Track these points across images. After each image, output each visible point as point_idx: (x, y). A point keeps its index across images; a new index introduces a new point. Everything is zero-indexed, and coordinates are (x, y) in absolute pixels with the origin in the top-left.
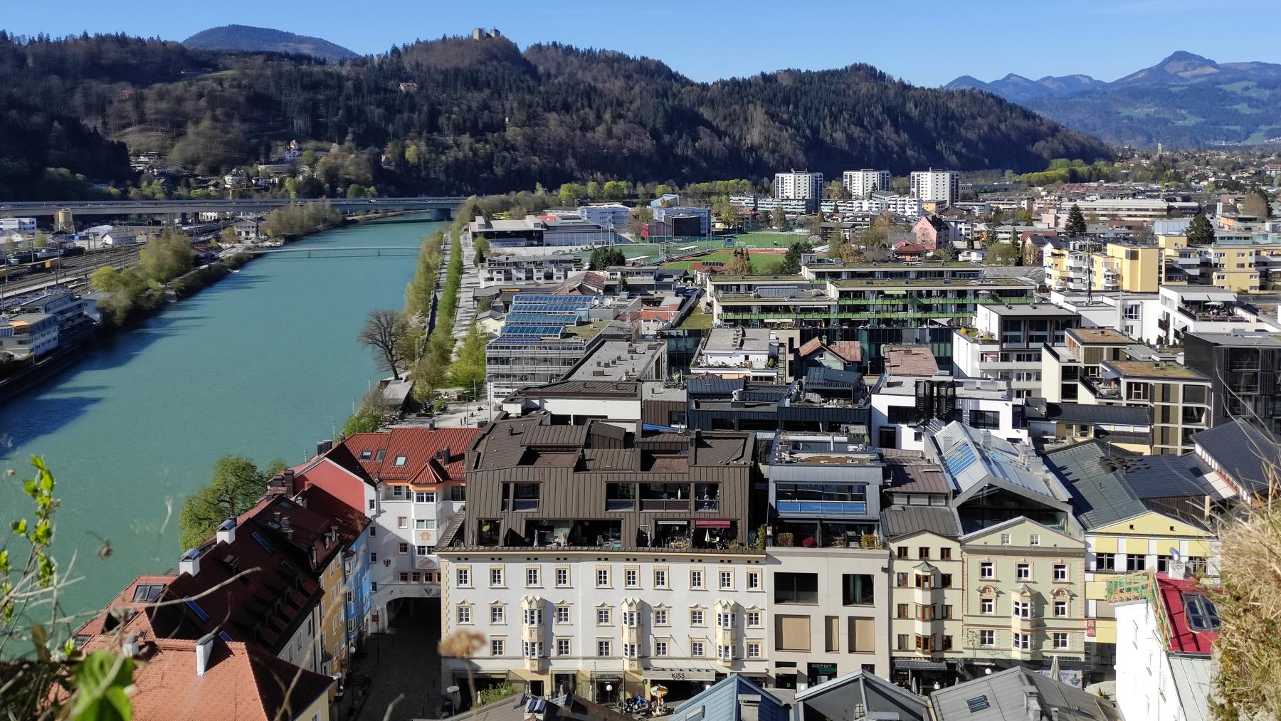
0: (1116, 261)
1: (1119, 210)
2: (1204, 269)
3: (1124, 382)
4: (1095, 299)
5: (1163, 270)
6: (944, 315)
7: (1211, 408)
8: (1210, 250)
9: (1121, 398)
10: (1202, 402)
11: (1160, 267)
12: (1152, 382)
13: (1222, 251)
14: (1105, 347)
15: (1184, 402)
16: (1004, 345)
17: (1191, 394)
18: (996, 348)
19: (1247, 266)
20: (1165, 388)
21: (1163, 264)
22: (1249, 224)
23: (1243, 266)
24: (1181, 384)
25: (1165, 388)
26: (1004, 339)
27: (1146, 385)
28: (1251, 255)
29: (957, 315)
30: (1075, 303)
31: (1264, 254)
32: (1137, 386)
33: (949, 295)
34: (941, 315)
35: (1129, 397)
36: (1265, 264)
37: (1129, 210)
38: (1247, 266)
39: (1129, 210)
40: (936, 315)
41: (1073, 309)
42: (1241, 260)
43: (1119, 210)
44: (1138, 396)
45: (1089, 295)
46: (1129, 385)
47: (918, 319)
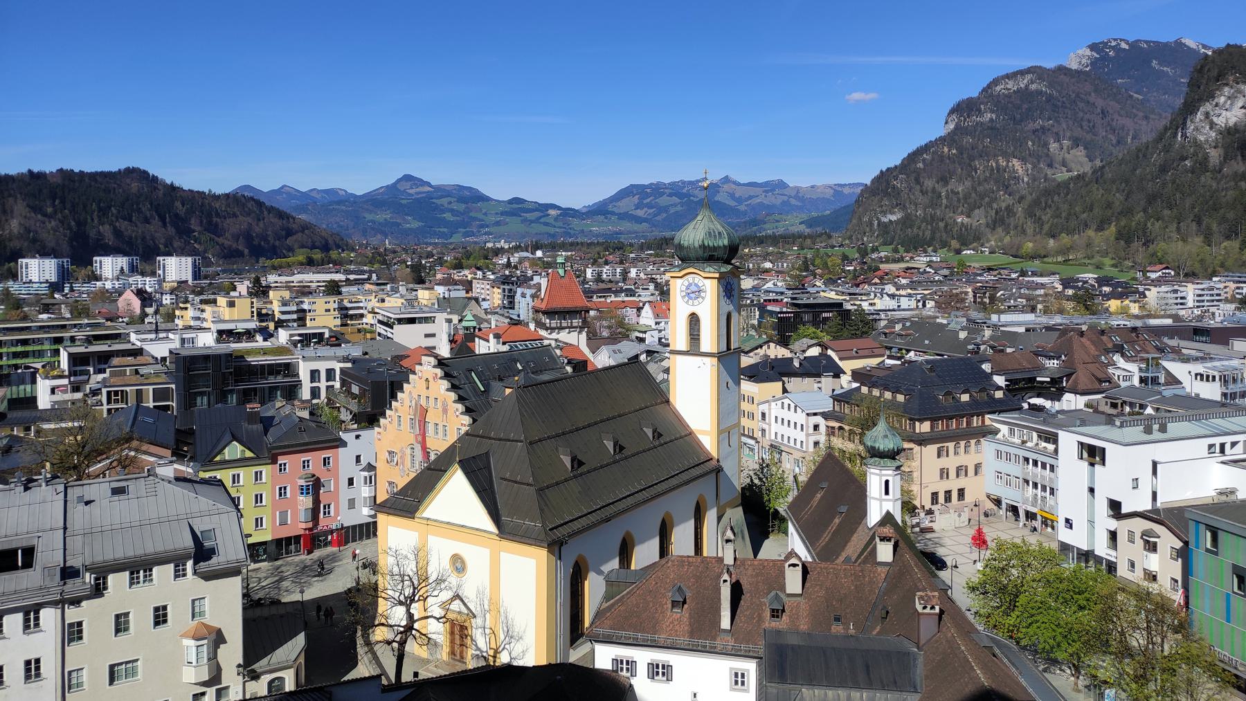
0: (221, 309)
1: (311, 282)
2: (301, 315)
3: (104, 391)
4: (162, 335)
5: (255, 314)
6: (40, 360)
7: (174, 405)
8: (306, 300)
9: (102, 405)
10: (168, 400)
11: (253, 312)
12: (128, 389)
13: (314, 300)
14: (128, 369)
15: (154, 401)
16: (72, 379)
17: (160, 395)
18: (65, 381)
19: (332, 310)
20: (139, 393)
21: (254, 310)
22: (382, 287)
23: (329, 310)
24: (151, 388)
25: (139, 393)
26: (73, 373)
27: (122, 391)
28: (335, 302)
29: (53, 359)
30: (141, 341)
31: (345, 301)
32: (116, 393)
33: (46, 342)
34: (36, 360)
35: (109, 402)
36: (347, 309)
37: (318, 282)
38: (332, 310)
39: (318, 282)
40: (31, 360)
41: (139, 344)
42: (327, 307)
43: (311, 282)
44: (117, 401)
45: (157, 333)
46: (109, 393)
47: (14, 365)
